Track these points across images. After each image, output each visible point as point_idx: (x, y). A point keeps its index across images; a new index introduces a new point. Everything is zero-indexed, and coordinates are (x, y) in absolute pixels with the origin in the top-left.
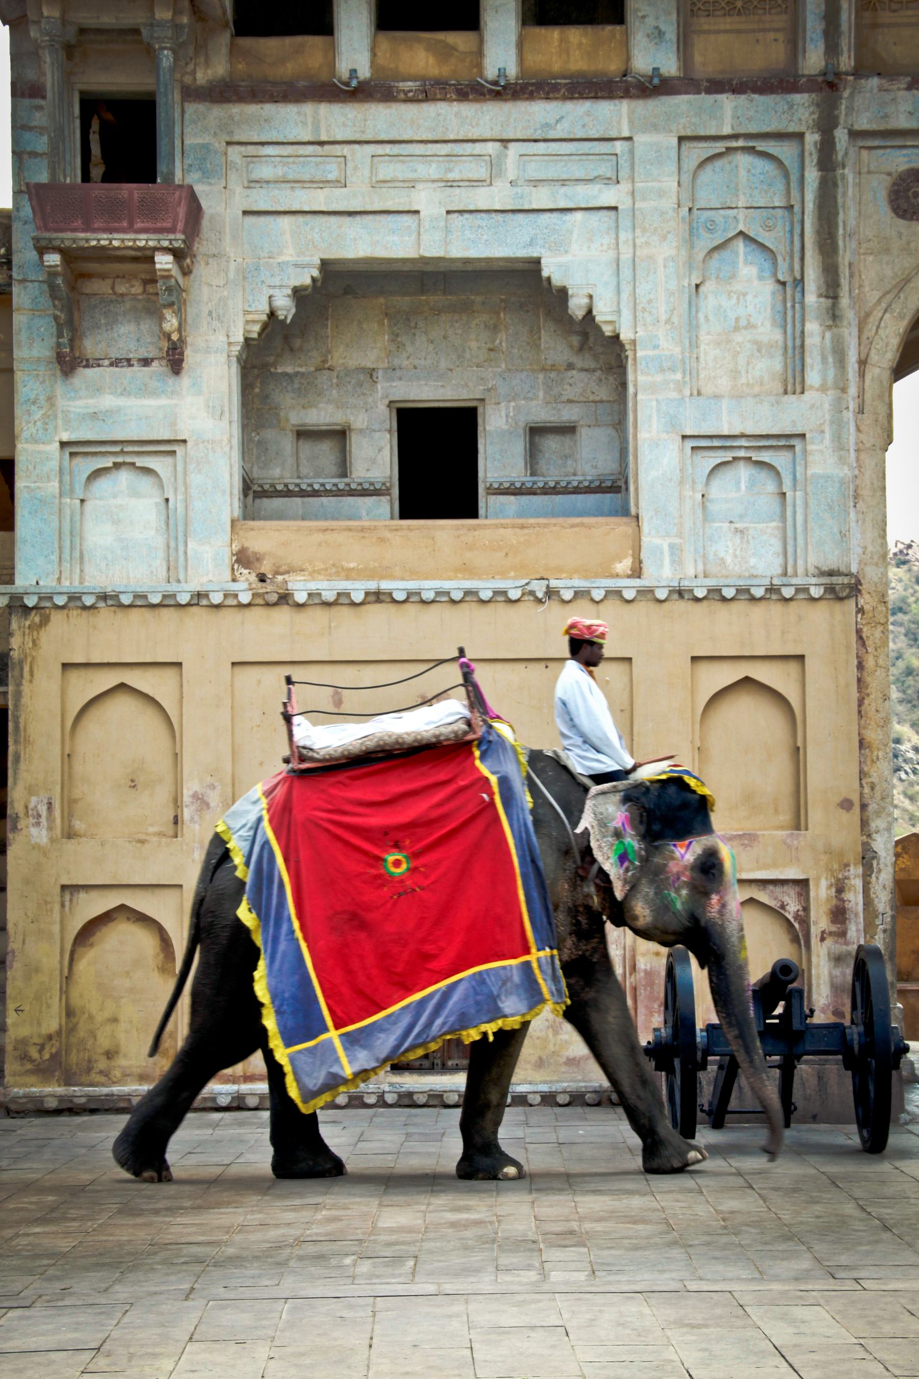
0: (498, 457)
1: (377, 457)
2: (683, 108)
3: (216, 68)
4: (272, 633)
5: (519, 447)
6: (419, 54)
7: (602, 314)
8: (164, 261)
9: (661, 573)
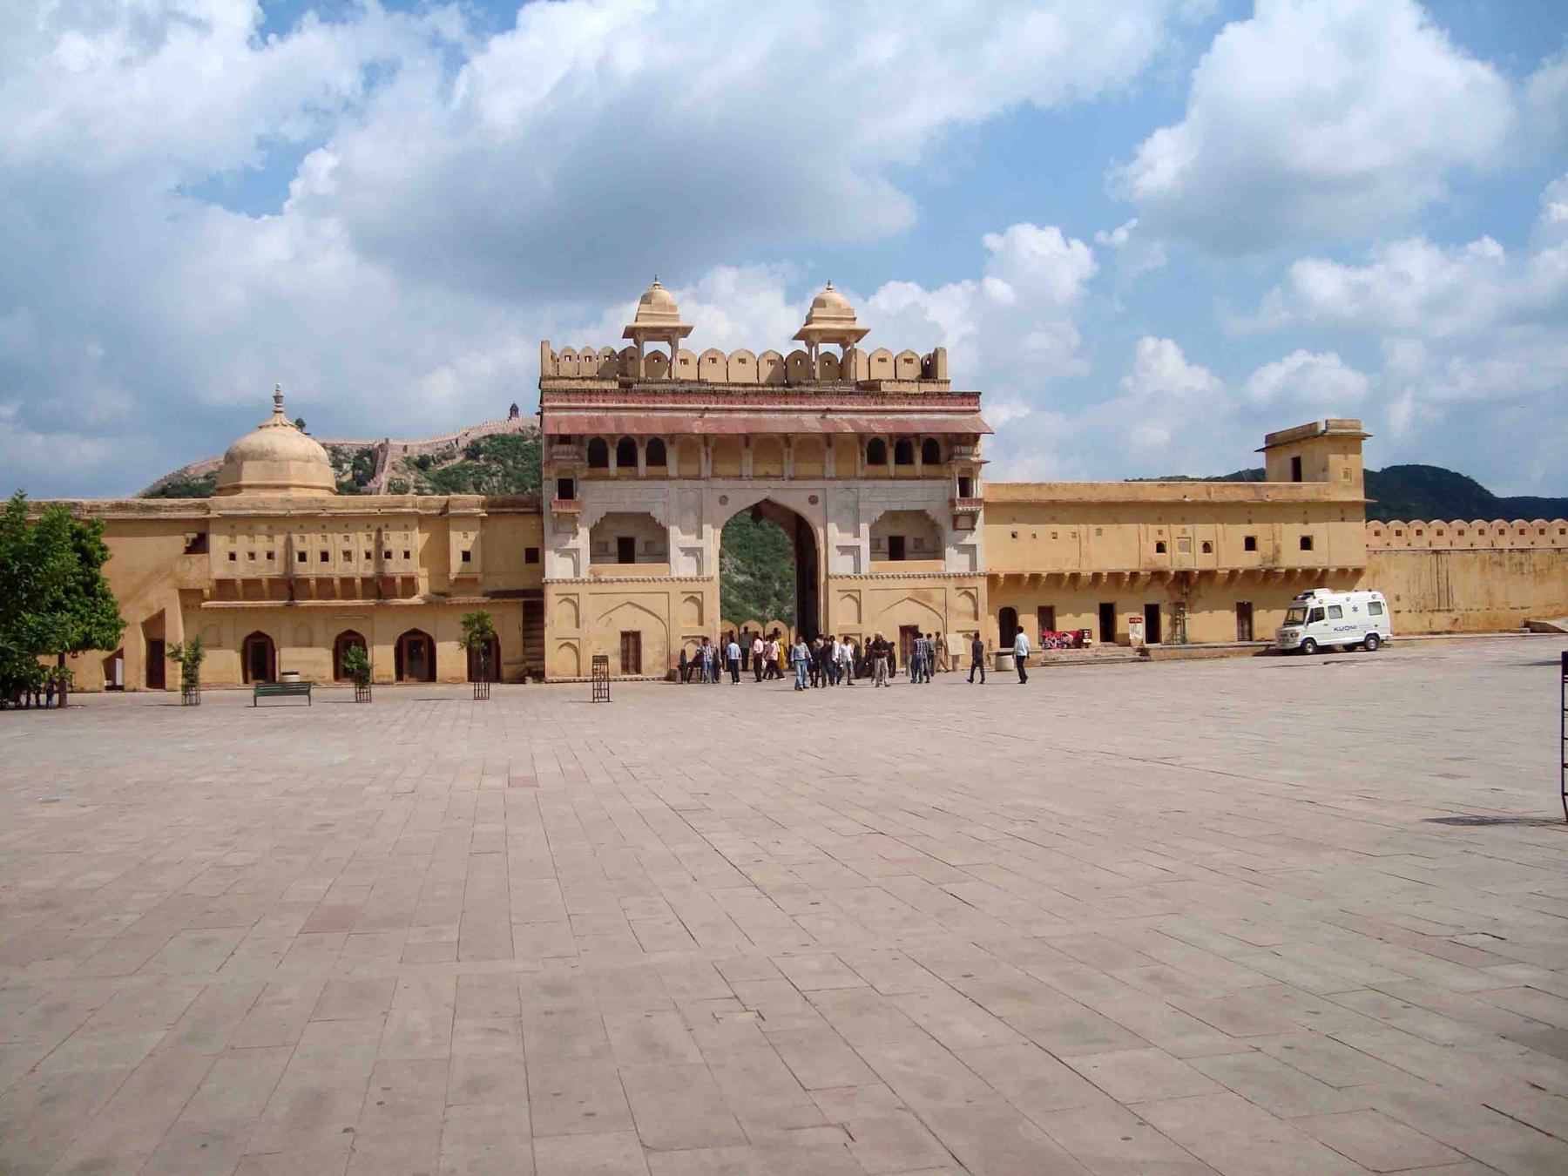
0: (639, 547)
1: (614, 548)
2: (679, 482)
3: (585, 473)
4: (597, 588)
6: (626, 471)
9: (675, 575)
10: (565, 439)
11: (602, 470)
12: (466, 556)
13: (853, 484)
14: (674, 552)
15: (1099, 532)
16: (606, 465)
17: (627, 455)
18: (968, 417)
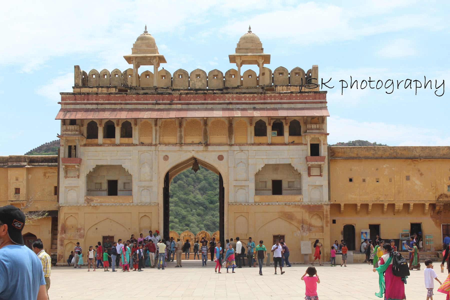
0: (120, 186)
1: (105, 186)
5: (123, 185)
6: (108, 141)
7: (129, 172)
8: (76, 167)
10: (73, 122)
11: (94, 141)
12: (17, 191)
13: (243, 148)
14: (135, 189)
15: (408, 178)
16: (96, 137)
17: (110, 132)
18: (320, 105)
